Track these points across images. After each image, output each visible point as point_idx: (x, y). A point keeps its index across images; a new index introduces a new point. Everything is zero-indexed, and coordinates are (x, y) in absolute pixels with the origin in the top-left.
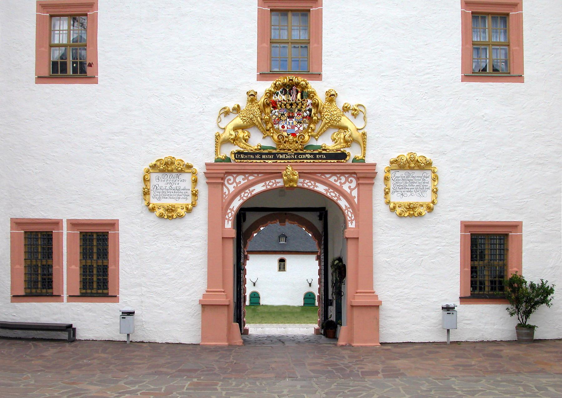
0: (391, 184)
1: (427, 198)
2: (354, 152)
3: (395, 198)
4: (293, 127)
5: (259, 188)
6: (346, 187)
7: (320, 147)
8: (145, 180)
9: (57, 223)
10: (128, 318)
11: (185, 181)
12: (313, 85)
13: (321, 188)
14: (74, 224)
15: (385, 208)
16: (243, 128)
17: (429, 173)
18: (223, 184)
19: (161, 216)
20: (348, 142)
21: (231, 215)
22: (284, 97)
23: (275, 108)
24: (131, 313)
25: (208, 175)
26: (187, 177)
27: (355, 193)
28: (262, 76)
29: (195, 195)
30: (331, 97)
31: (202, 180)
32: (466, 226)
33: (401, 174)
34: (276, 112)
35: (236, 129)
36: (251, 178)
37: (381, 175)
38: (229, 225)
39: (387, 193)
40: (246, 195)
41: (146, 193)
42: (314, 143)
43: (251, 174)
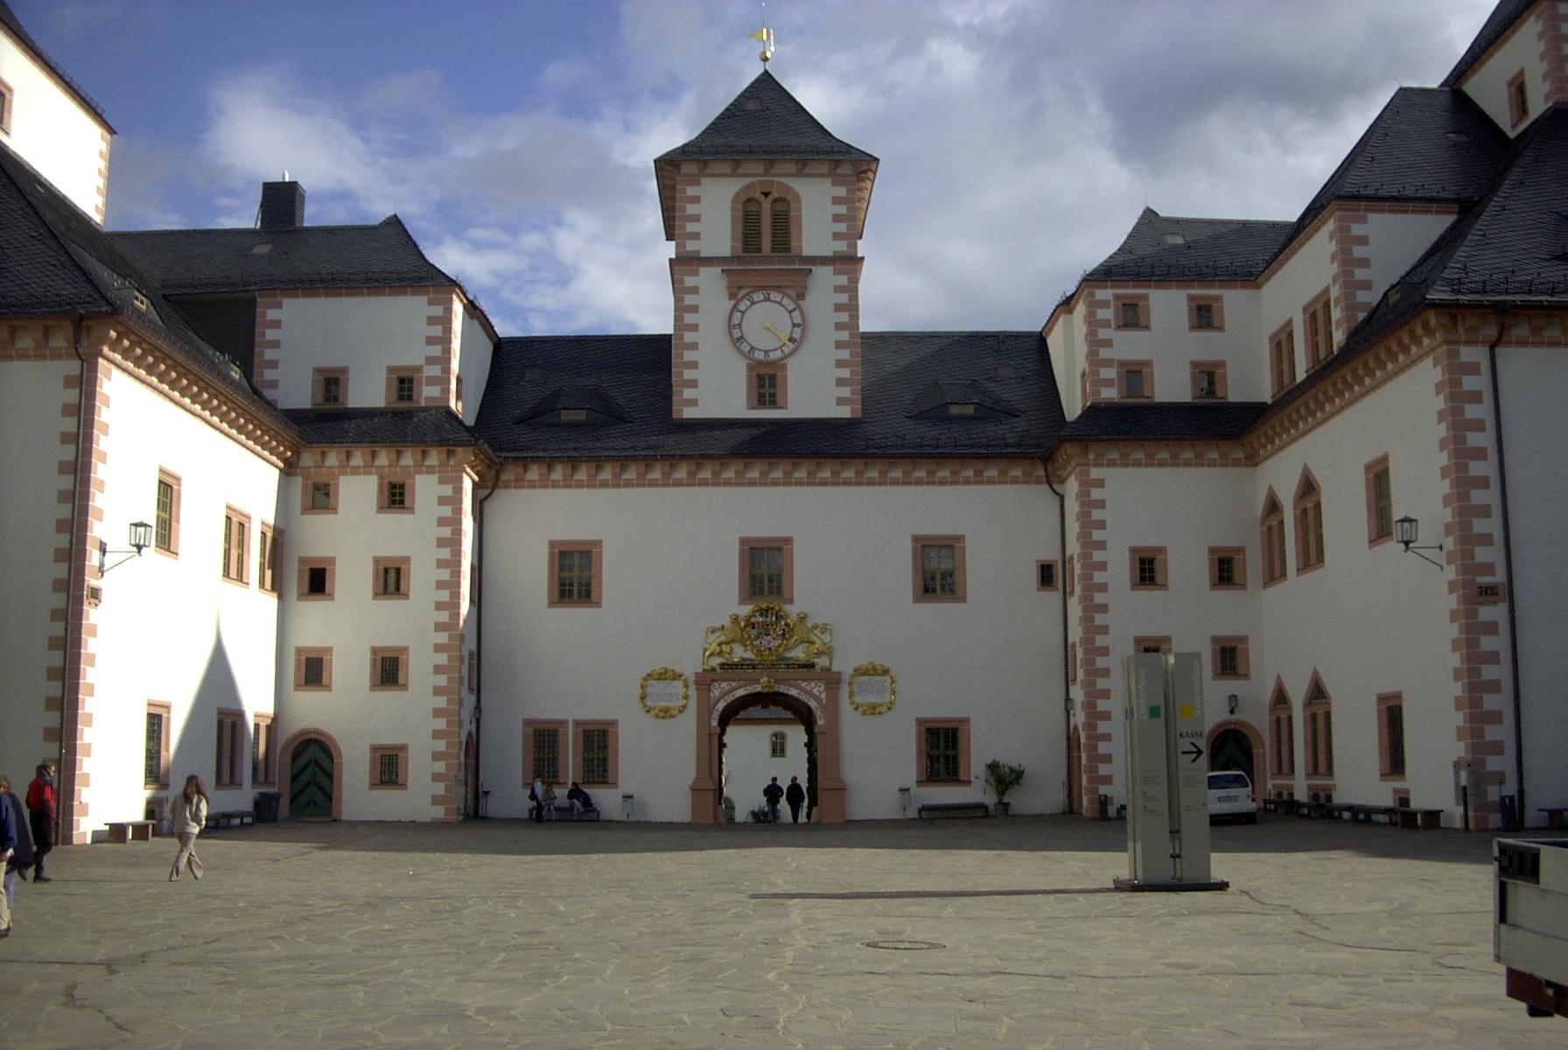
0: (855, 688)
1: (887, 698)
2: (822, 662)
3: (858, 699)
4: (769, 642)
5: (740, 693)
6: (815, 691)
7: (791, 659)
8: (642, 687)
9: (563, 723)
10: (630, 800)
11: (678, 687)
12: (787, 608)
13: (794, 692)
14: (577, 723)
15: (851, 707)
16: (726, 643)
17: (888, 678)
18: (710, 690)
19: (657, 716)
20: (820, 654)
21: (716, 715)
22: (761, 619)
23: (753, 628)
24: (631, 797)
25: (696, 683)
26: (679, 684)
27: (823, 696)
28: (743, 601)
29: (686, 697)
30: (803, 618)
31: (692, 687)
32: (920, 722)
33: (864, 678)
34: (755, 632)
35: (720, 644)
36: (734, 684)
37: (846, 678)
38: (715, 723)
39: (851, 696)
40: (730, 698)
41: (643, 698)
42: (788, 655)
43: (734, 681)
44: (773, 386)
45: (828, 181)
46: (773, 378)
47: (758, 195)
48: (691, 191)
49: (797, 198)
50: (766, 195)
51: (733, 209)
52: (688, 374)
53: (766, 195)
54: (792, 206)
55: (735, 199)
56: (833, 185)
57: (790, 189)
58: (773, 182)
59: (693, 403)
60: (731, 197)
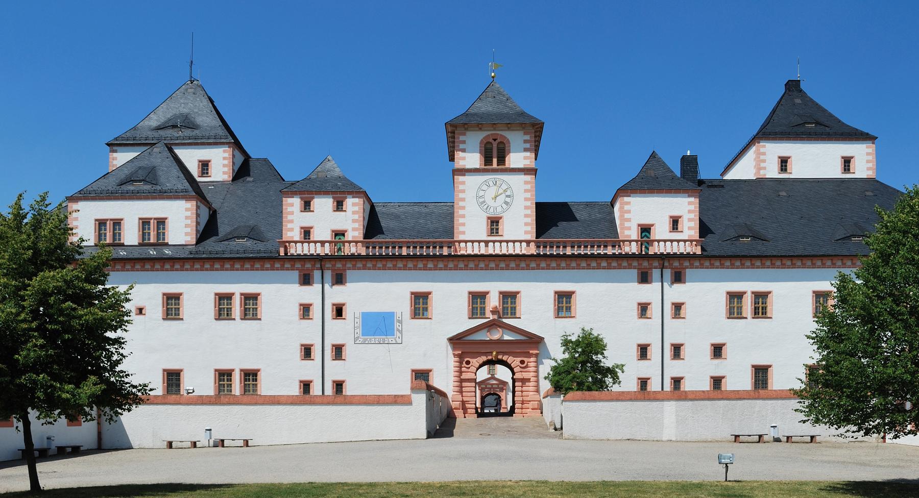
44: (497, 225)
45: (521, 133)
46: (497, 222)
47: (491, 140)
48: (462, 138)
49: (509, 142)
50: (495, 140)
51: (480, 147)
52: (461, 220)
53: (495, 140)
54: (506, 145)
55: (481, 142)
56: (524, 134)
57: (505, 137)
58: (498, 134)
59: (463, 233)
60: (479, 142)
